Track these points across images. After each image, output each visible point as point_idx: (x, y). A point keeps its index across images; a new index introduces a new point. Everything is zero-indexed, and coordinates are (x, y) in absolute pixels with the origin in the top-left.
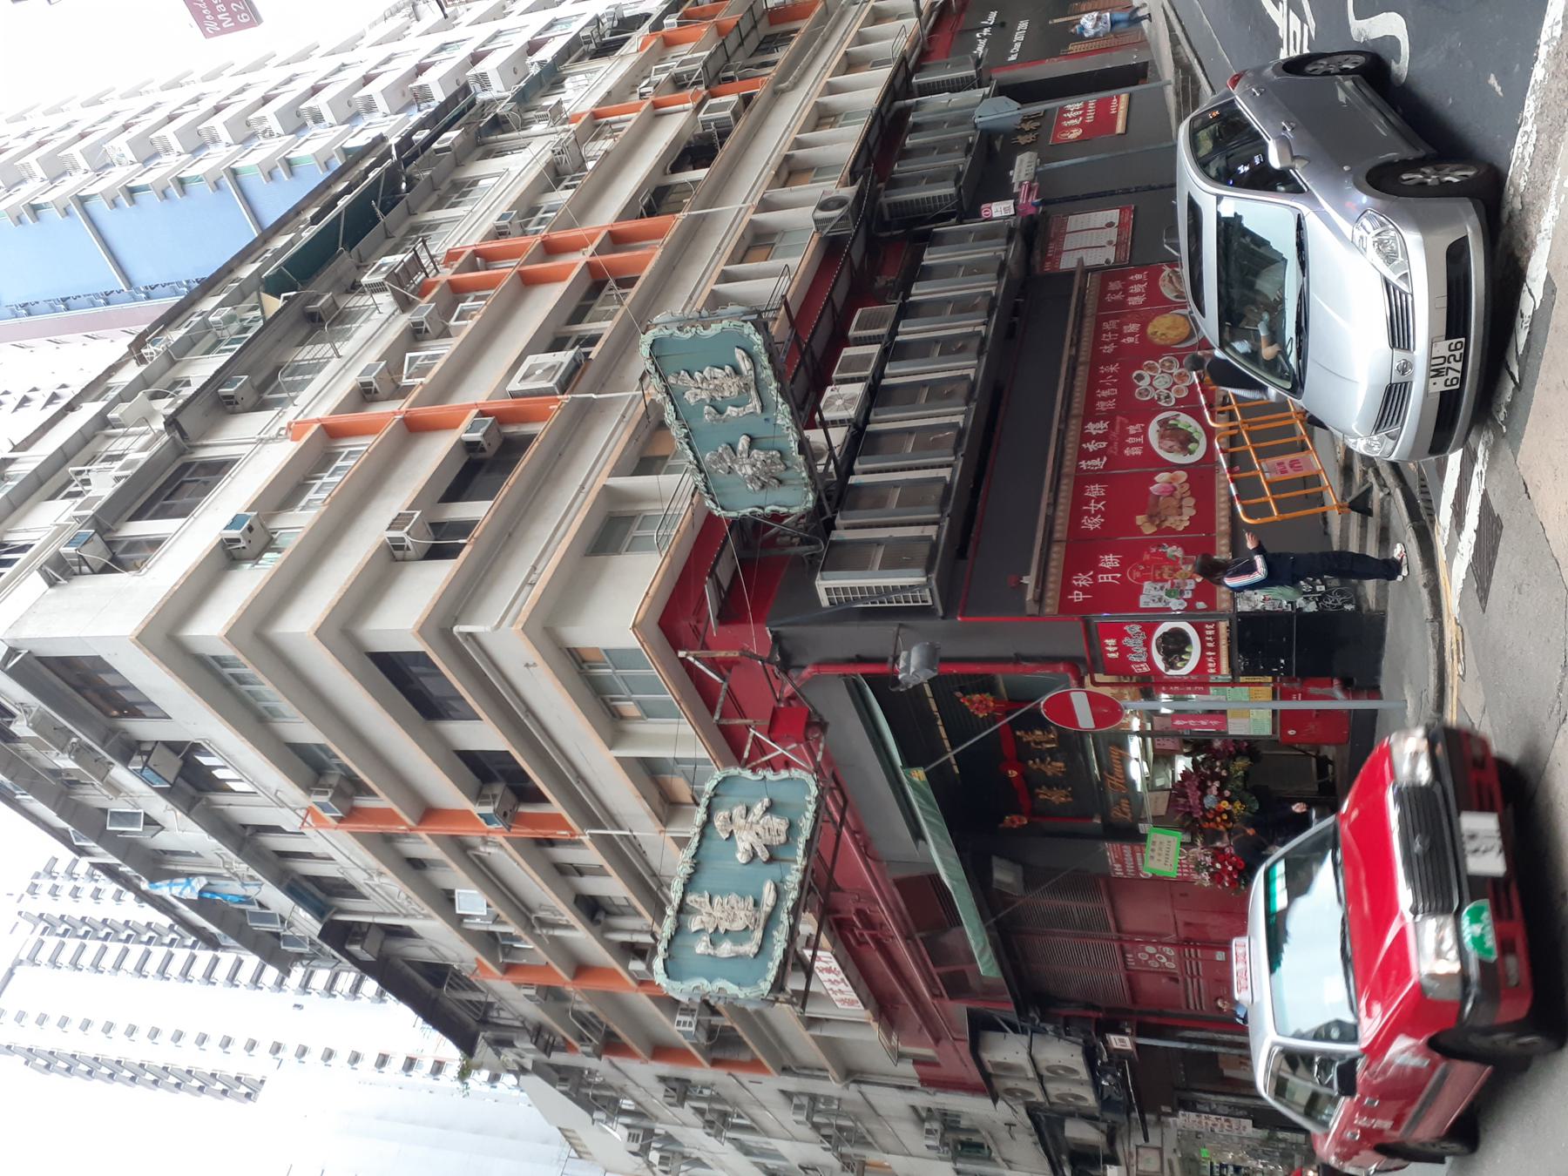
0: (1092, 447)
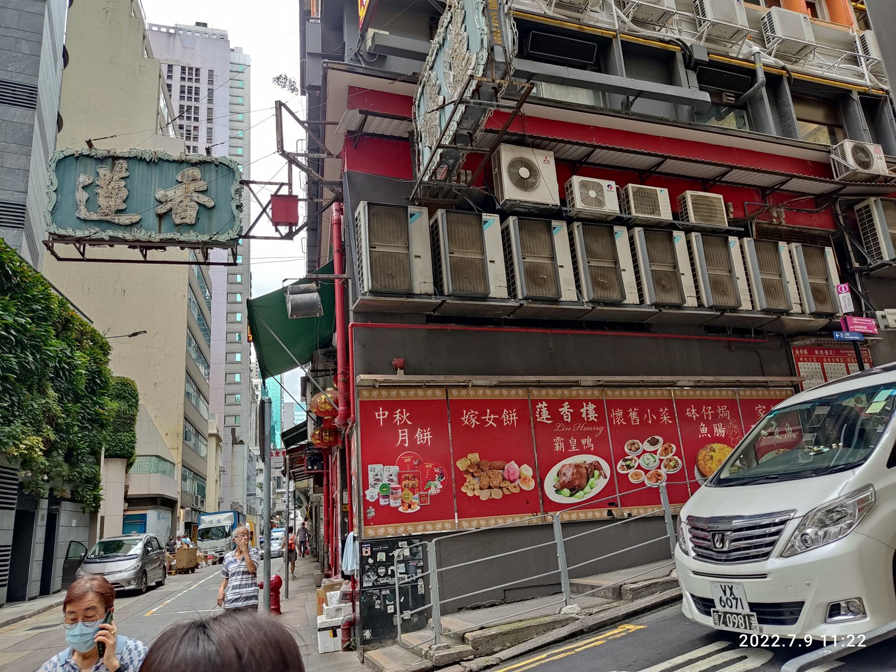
0: (565, 410)
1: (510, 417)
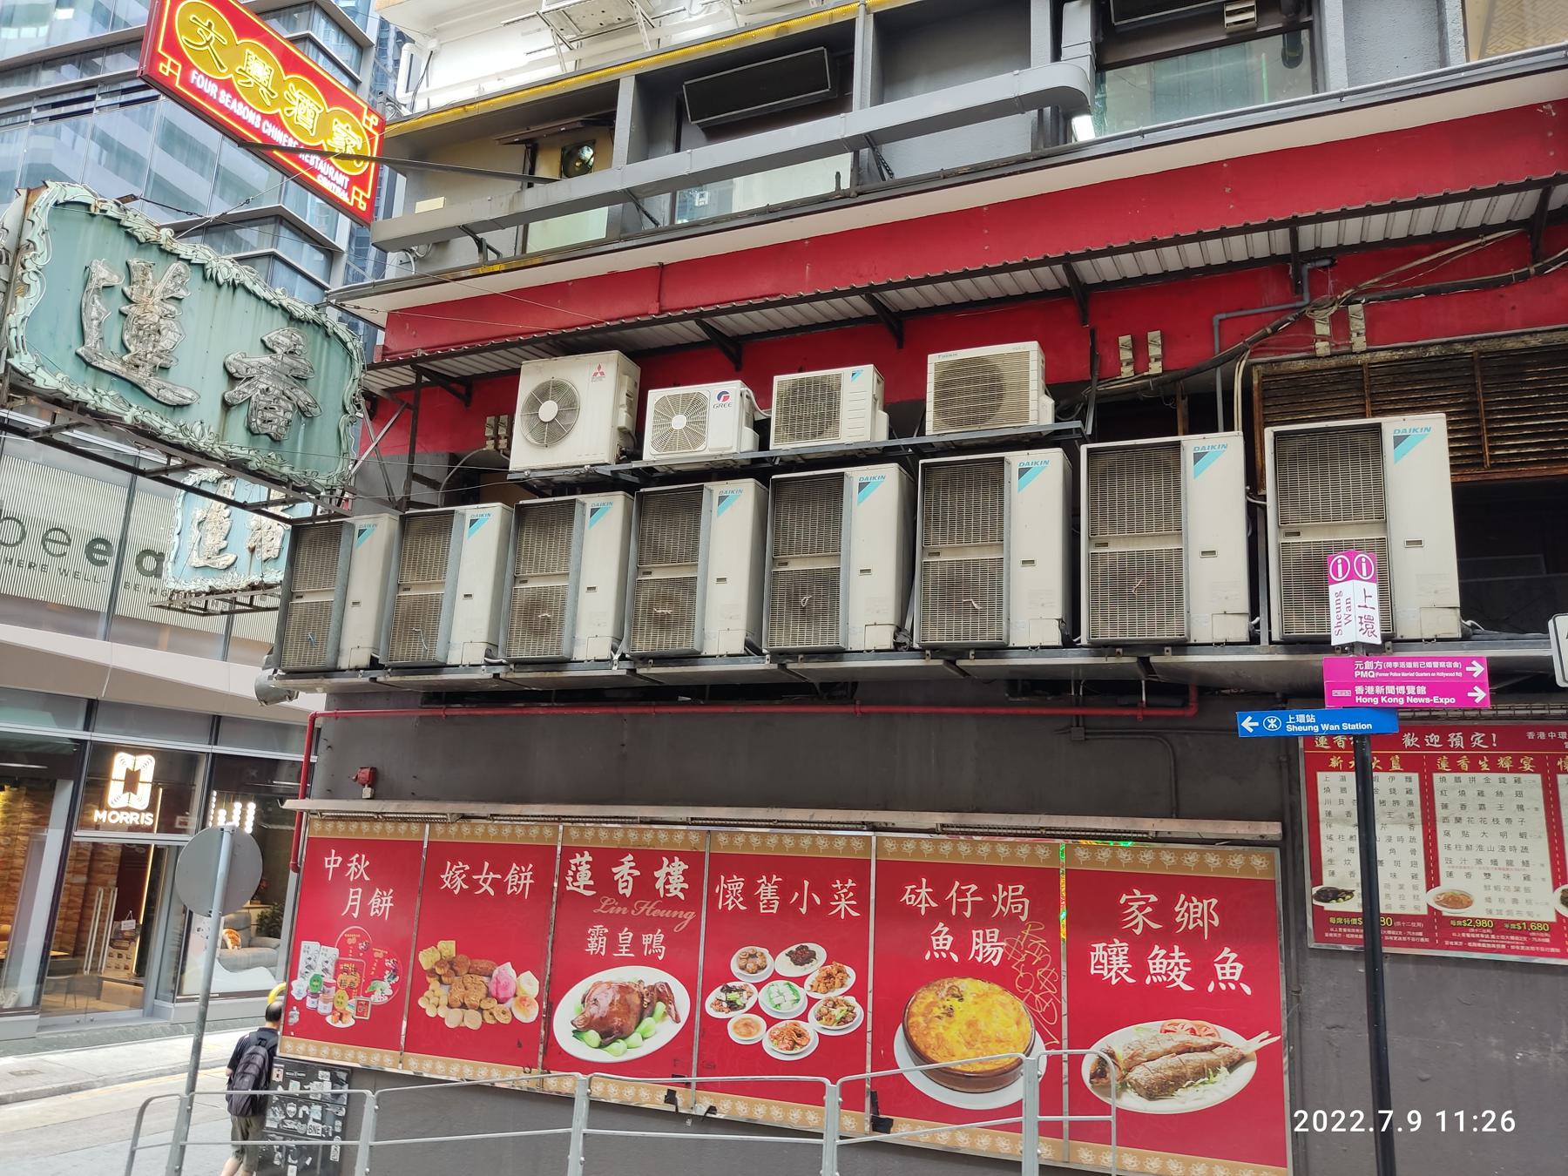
0: (625, 872)
1: (520, 879)
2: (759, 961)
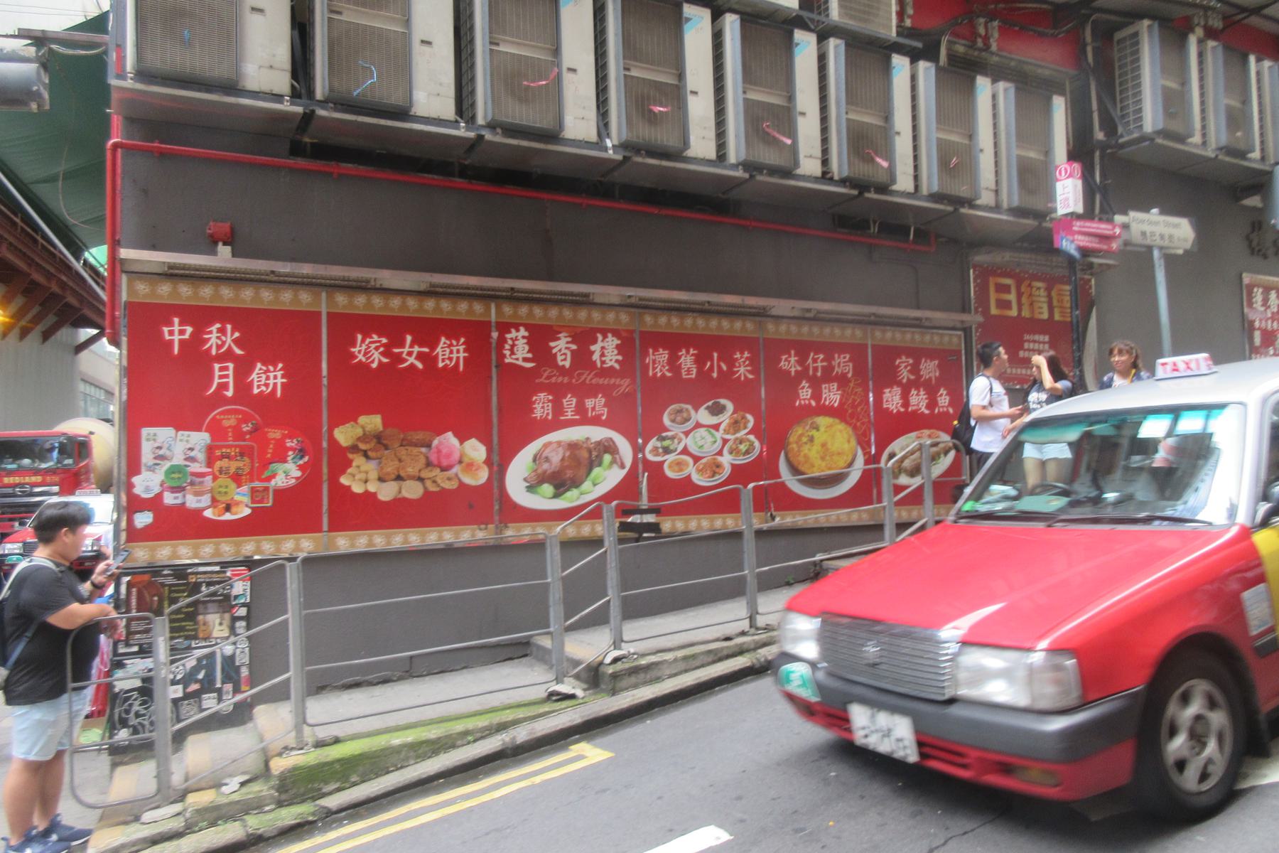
0: (562, 347)
1: (451, 353)
2: (685, 415)
